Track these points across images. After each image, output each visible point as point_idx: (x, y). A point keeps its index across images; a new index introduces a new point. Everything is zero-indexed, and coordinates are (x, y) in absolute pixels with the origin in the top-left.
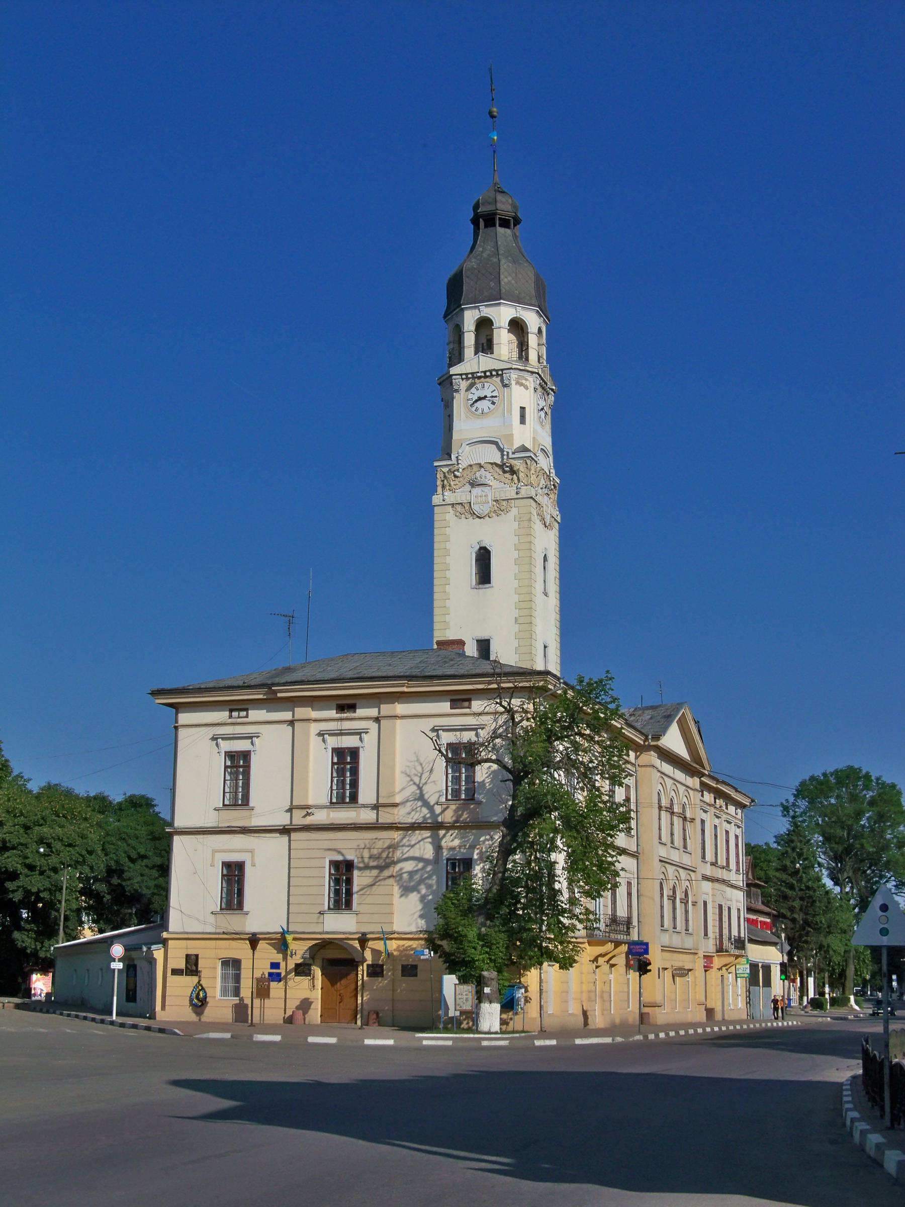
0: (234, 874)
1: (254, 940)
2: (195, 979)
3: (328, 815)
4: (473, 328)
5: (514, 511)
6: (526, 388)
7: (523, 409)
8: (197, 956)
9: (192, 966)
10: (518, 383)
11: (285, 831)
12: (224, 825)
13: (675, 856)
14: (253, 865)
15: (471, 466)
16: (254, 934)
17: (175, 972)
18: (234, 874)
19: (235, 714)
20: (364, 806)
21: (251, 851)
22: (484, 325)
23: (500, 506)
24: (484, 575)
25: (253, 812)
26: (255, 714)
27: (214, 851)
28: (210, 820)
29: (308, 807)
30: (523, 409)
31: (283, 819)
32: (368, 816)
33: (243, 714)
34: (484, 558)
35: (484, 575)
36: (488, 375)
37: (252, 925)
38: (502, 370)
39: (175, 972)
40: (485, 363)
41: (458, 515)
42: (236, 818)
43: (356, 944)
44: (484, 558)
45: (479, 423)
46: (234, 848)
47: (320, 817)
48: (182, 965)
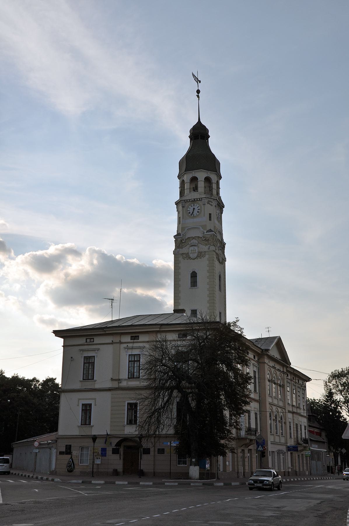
0: (87, 409)
1: (94, 438)
2: (70, 456)
4: (189, 181)
5: (207, 256)
6: (212, 205)
7: (210, 214)
8: (70, 446)
9: (68, 450)
10: (208, 203)
11: (109, 390)
13: (275, 402)
14: (96, 405)
16: (95, 436)
17: (61, 453)
18: (87, 409)
21: (95, 399)
22: (194, 179)
23: (200, 255)
24: (194, 283)
26: (97, 340)
27: (79, 399)
29: (119, 380)
30: (210, 214)
31: (109, 385)
33: (92, 340)
34: (194, 275)
35: (194, 283)
36: (194, 201)
37: (94, 432)
39: (61, 453)
40: (195, 195)
41: (184, 258)
42: (89, 385)
43: (138, 439)
44: (194, 275)
46: (87, 398)
47: (124, 384)
48: (64, 449)
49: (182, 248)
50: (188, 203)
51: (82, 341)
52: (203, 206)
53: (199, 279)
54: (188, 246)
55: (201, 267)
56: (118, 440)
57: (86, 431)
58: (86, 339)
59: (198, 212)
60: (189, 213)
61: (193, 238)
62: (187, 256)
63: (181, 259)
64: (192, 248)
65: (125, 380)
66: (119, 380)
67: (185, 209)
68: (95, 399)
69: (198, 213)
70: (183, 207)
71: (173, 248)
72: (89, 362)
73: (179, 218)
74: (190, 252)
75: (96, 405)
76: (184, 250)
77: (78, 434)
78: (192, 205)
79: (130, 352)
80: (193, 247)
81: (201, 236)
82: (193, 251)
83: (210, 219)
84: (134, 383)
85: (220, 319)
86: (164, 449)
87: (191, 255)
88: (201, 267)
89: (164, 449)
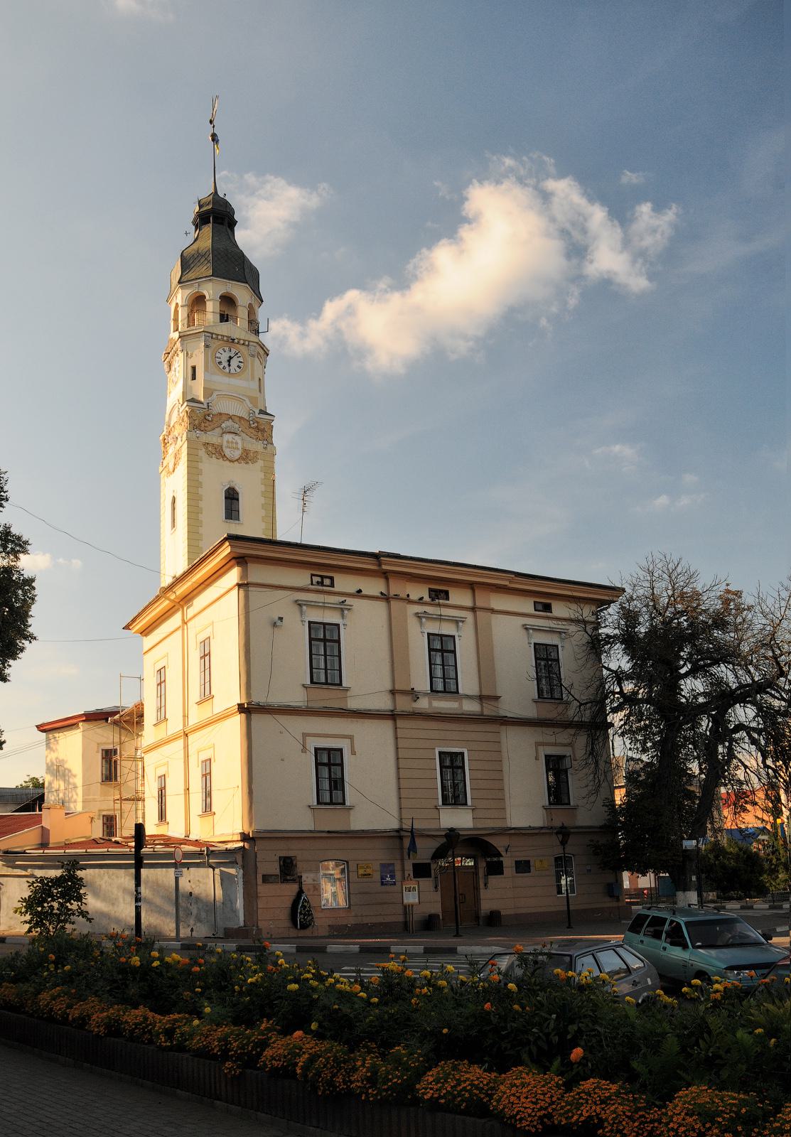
2: (291, 889)
3: (430, 703)
5: (260, 463)
11: (393, 716)
12: (317, 705)
14: (353, 753)
15: (220, 414)
19: (316, 579)
20: (468, 697)
21: (351, 738)
23: (246, 457)
25: (349, 694)
26: (345, 583)
27: (305, 735)
28: (297, 697)
31: (384, 703)
32: (471, 707)
34: (232, 496)
38: (249, 342)
41: (210, 454)
42: (326, 698)
44: (232, 496)
45: (226, 380)
46: (328, 732)
47: (423, 704)
48: (274, 869)
49: (205, 431)
50: (218, 343)
51: (301, 578)
52: (250, 359)
53: (244, 504)
54: (218, 431)
56: (435, 844)
57: (331, 820)
58: (312, 575)
59: (239, 367)
60: (220, 363)
61: (230, 417)
62: (218, 452)
63: (202, 453)
65: (426, 694)
66: (414, 694)
67: (210, 351)
68: (351, 738)
69: (238, 370)
70: (207, 346)
72: (325, 640)
74: (225, 444)
75: (353, 753)
76: (212, 437)
77: (312, 828)
78: (227, 349)
79: (434, 628)
80: (233, 435)
81: (246, 417)
84: (445, 705)
86: (528, 862)
87: (227, 452)
89: (528, 862)
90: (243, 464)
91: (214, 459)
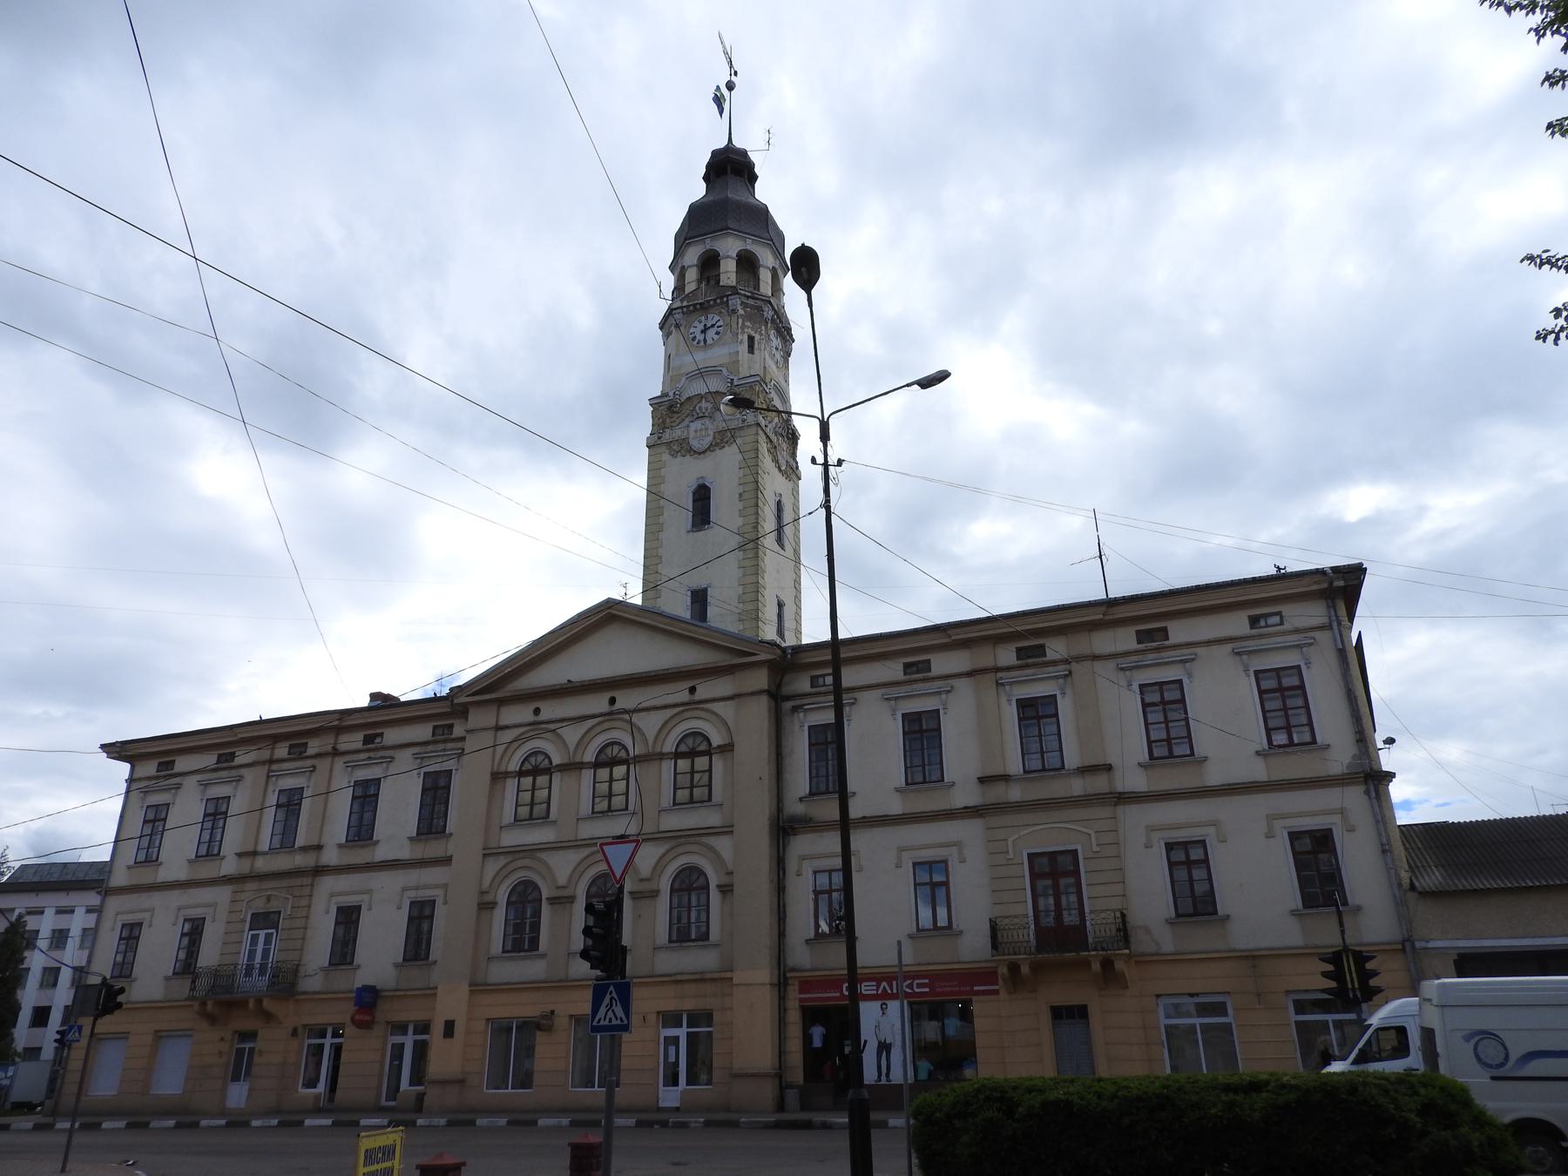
23: (723, 439)
34: (702, 496)
41: (674, 455)
44: (702, 496)
55: (723, 470)
62: (683, 448)
63: (666, 457)
64: (697, 425)
71: (648, 429)
73: (668, 358)
74: (692, 434)
82: (698, 432)
83: (751, 349)
85: (780, 633)
87: (695, 444)
88: (723, 470)
90: (718, 452)
91: (679, 458)
